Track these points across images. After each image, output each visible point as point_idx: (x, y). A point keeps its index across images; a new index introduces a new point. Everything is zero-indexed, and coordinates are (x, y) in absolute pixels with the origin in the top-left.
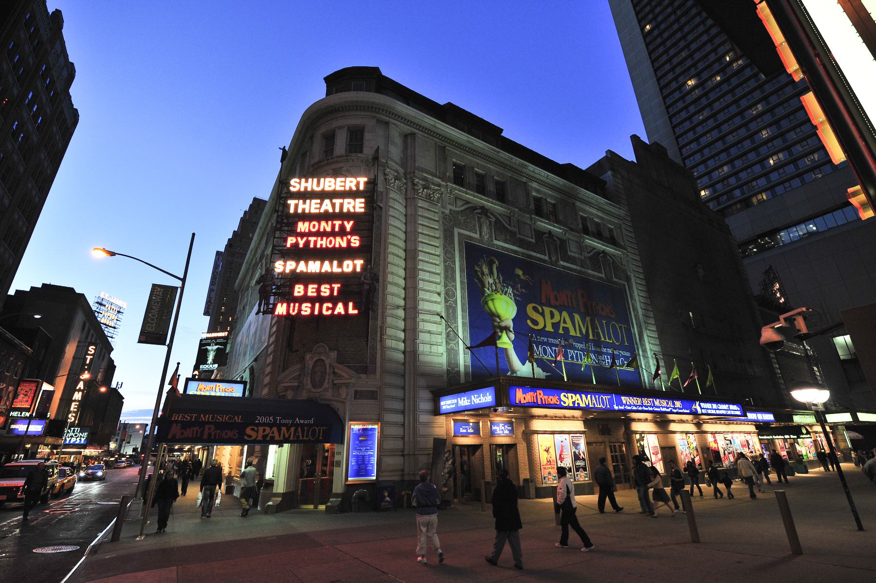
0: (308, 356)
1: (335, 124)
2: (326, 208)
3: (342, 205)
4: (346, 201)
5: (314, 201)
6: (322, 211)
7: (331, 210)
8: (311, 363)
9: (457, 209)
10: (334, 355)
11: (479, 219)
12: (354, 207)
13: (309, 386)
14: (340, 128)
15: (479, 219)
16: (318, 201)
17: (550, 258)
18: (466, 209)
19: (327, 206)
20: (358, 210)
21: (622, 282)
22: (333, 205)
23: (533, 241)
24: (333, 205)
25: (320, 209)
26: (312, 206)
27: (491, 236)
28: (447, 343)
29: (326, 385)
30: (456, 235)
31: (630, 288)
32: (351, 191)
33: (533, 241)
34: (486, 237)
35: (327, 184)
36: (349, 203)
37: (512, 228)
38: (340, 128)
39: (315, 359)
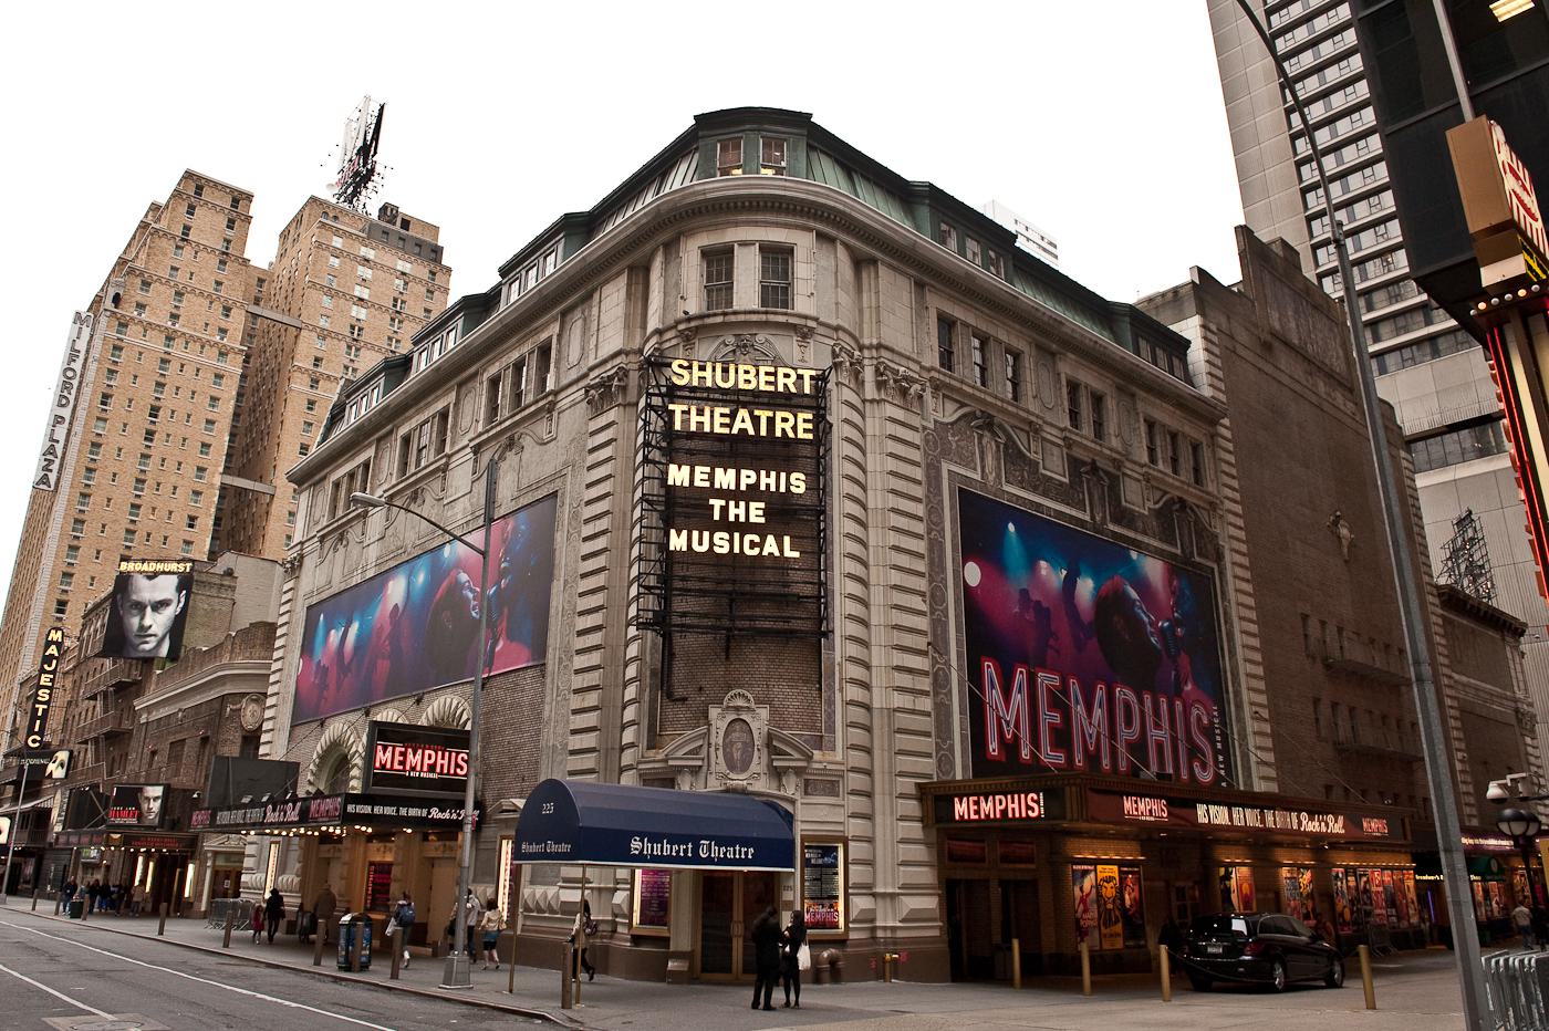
0: (714, 712)
1: (732, 235)
2: (743, 426)
3: (771, 421)
4: (780, 415)
5: (718, 411)
6: (735, 431)
7: (751, 432)
8: (723, 725)
9: (946, 420)
10: (764, 713)
11: (981, 437)
12: (794, 428)
13: (723, 767)
14: (744, 244)
15: (981, 437)
16: (727, 411)
17: (1093, 518)
18: (959, 419)
19: (743, 422)
20: (801, 435)
21: (1209, 564)
22: (756, 421)
23: (1066, 480)
25: (730, 426)
26: (713, 420)
27: (998, 476)
28: (936, 694)
29: (754, 767)
30: (945, 475)
31: (1222, 573)
32: (787, 395)
33: (1066, 480)
34: (991, 478)
35: (742, 376)
36: (785, 420)
37: (1032, 456)
38: (744, 244)
39: (731, 717)
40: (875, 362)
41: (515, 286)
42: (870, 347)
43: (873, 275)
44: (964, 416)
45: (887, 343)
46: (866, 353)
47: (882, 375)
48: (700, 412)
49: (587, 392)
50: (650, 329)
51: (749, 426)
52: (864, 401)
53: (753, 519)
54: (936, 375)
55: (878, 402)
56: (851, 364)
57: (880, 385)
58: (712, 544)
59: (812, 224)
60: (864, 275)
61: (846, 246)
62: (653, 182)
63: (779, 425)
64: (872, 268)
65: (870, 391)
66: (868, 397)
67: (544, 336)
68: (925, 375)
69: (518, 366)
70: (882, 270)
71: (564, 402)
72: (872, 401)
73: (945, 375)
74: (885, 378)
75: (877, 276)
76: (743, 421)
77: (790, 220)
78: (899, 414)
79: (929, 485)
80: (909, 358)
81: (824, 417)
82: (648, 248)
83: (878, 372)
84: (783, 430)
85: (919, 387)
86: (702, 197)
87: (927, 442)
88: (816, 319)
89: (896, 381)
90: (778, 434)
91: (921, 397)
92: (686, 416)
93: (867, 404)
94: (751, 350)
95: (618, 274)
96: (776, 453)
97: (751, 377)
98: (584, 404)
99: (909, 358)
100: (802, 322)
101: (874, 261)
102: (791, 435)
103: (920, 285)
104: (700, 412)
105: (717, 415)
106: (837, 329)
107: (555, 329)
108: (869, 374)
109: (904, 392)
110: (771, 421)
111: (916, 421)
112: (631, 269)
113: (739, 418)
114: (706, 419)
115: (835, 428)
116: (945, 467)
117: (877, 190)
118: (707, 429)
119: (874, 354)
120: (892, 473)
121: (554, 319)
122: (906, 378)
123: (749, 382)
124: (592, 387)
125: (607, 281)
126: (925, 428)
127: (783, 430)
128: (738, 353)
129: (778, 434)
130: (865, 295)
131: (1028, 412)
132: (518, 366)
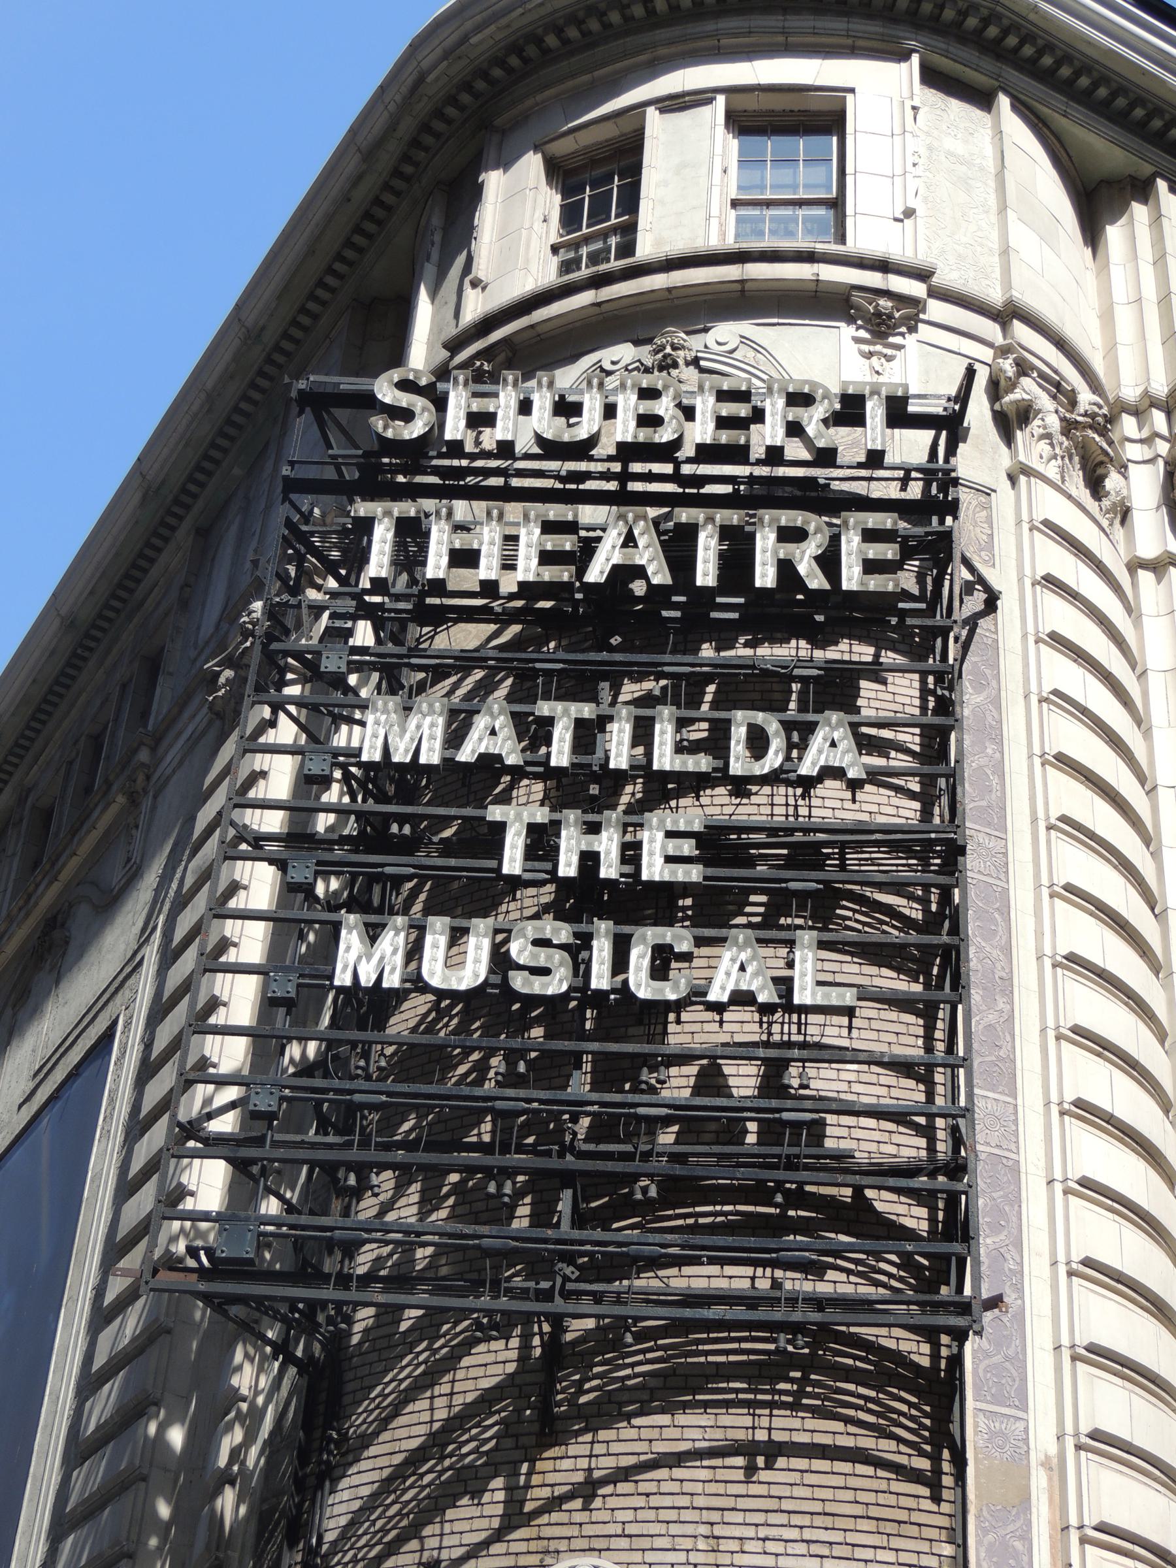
6: (596, 573)
12: (829, 562)
36: (792, 535)
53: (654, 869)
58: (501, 961)
63: (766, 551)
75: (1157, 218)
84: (786, 568)
88: (922, 275)
90: (765, 576)
100: (873, 279)
102: (817, 581)
106: (1007, 314)
115: (1007, 605)
127: (786, 568)
129: (765, 576)
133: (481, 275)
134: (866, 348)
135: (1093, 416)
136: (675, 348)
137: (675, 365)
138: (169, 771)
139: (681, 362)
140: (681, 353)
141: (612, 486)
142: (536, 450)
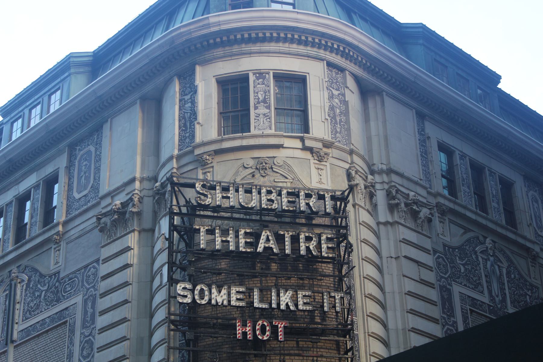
3: (295, 240)
6: (260, 249)
14: (261, 74)
22: (280, 239)
24: (280, 239)
25: (255, 245)
40: (386, 187)
41: (18, 125)
42: (381, 172)
43: (379, 106)
44: (468, 241)
45: (395, 169)
46: (378, 178)
47: (394, 198)
48: (225, 232)
49: (99, 219)
50: (164, 156)
51: (272, 244)
52: (378, 223)
54: (442, 201)
55: (392, 224)
56: (366, 187)
57: (392, 208)
59: (322, 53)
60: (371, 105)
61: (357, 79)
62: (162, 19)
64: (378, 99)
65: (384, 215)
66: (382, 219)
67: (49, 170)
68: (433, 201)
69: (22, 200)
70: (388, 101)
71: (72, 232)
72: (386, 224)
73: (450, 200)
74: (396, 201)
76: (268, 240)
77: (301, 49)
78: (412, 237)
79: (443, 307)
80: (416, 183)
81: (345, 237)
82: (160, 80)
83: (389, 195)
84: (308, 248)
85: (428, 211)
86: (216, 29)
87: (439, 264)
89: (406, 205)
90: (303, 252)
91: (430, 221)
92: (210, 237)
93: (381, 227)
94: (269, 172)
95: (133, 104)
96: (301, 269)
97: (273, 196)
98: (96, 231)
99: (416, 183)
101: (378, 92)
103: (421, 117)
104: (225, 232)
105: (242, 232)
107: (62, 162)
108: (380, 197)
109: (415, 215)
110: (295, 240)
111: (427, 244)
112: (144, 99)
113: (263, 238)
114: (231, 238)
116: (457, 289)
117: (374, 30)
118: (232, 248)
119: (386, 179)
120: (410, 293)
121: (60, 153)
122: (416, 202)
123: (272, 201)
124: (105, 215)
125: (120, 111)
126: (435, 252)
127: (308, 248)
128: (257, 175)
129: (303, 252)
130: (372, 124)
131: (525, 238)
132: (22, 200)
133: (200, 122)
134: (317, 166)
135: (372, 183)
136: (266, 164)
137: (266, 169)
138: (73, 237)
139: (267, 168)
140: (267, 165)
141: (258, 218)
142: (239, 207)
